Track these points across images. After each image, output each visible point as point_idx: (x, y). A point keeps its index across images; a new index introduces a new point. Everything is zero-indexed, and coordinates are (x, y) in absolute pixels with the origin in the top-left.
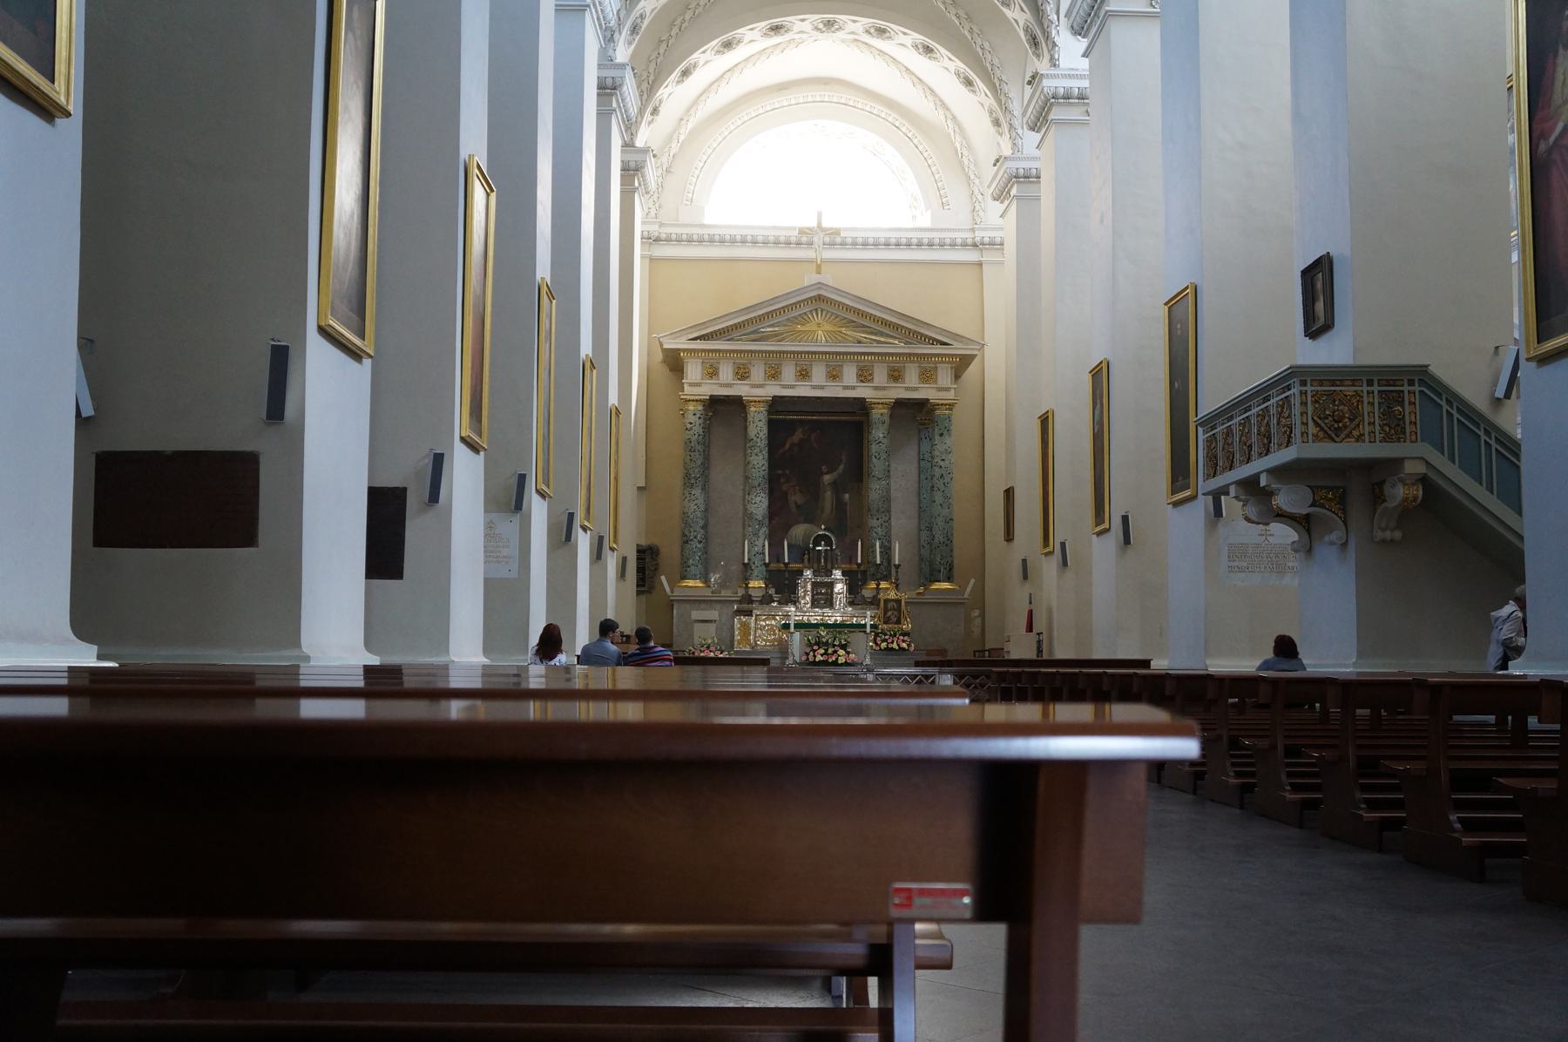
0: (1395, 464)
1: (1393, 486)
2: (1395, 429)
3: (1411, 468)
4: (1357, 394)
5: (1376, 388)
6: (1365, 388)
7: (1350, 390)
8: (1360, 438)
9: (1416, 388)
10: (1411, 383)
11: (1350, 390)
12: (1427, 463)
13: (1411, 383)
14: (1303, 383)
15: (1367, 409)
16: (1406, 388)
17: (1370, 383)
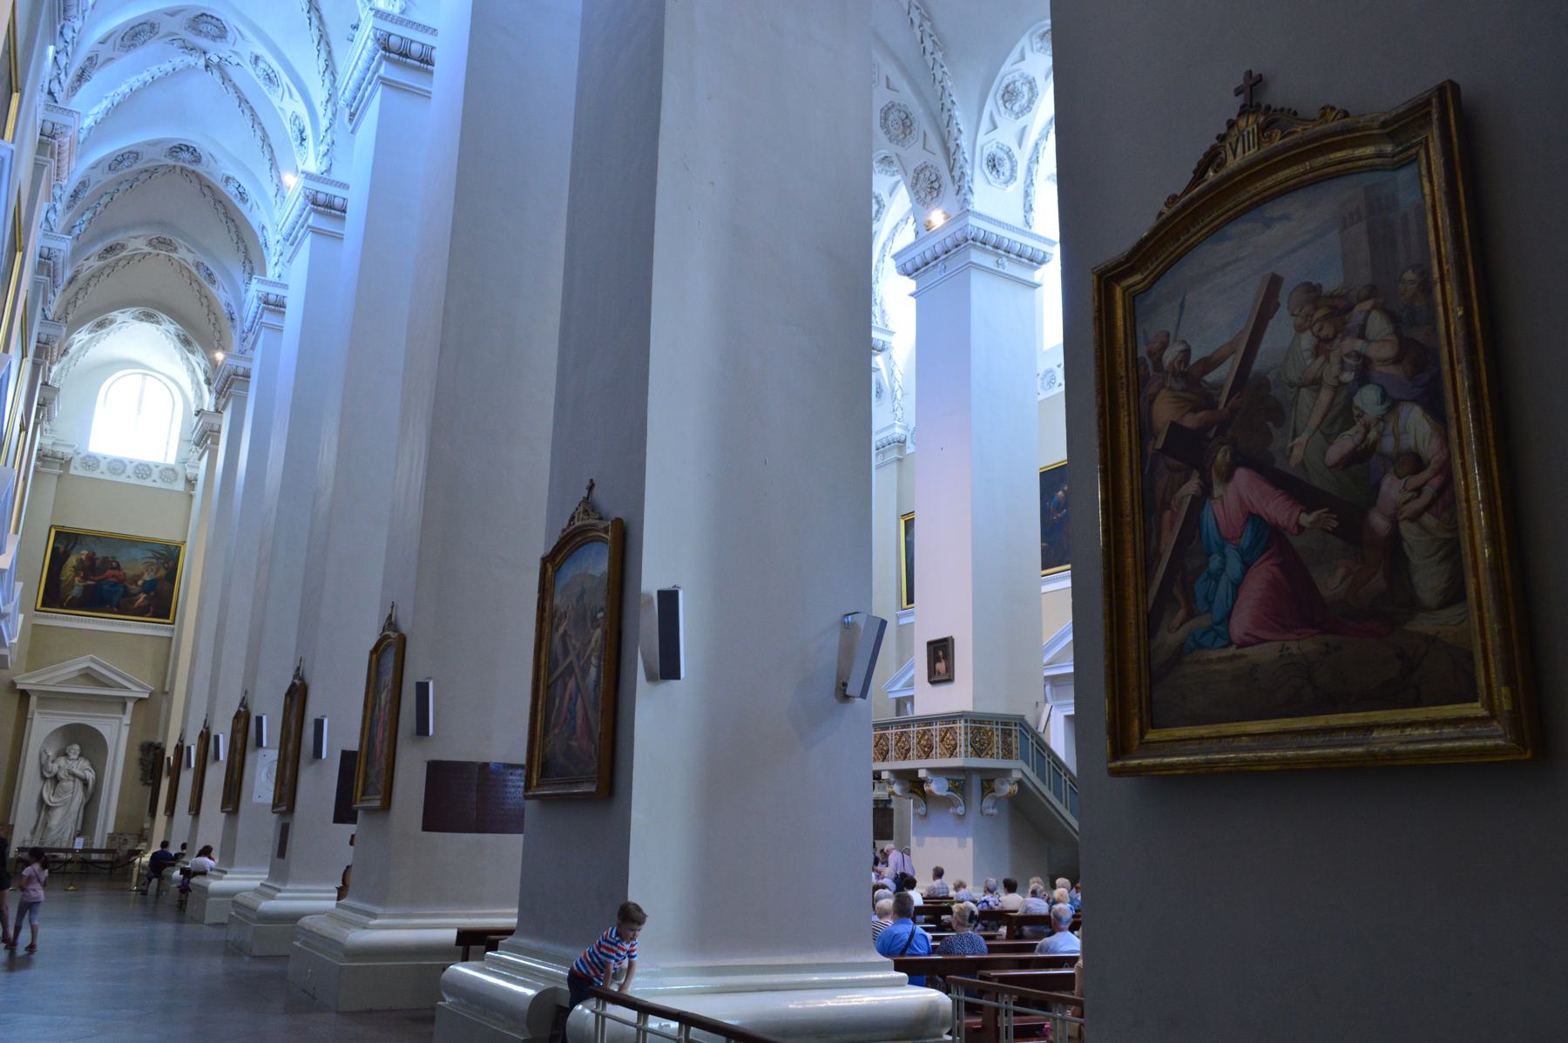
0: (1005, 773)
1: (1003, 784)
2: (1008, 754)
3: (1016, 775)
4: (991, 730)
5: (1000, 727)
6: (995, 726)
7: (988, 727)
8: (992, 756)
9: (1018, 728)
10: (1016, 725)
11: (988, 727)
12: (1022, 772)
13: (1016, 725)
14: (966, 721)
15: (995, 738)
16: (1013, 728)
17: (997, 723)
